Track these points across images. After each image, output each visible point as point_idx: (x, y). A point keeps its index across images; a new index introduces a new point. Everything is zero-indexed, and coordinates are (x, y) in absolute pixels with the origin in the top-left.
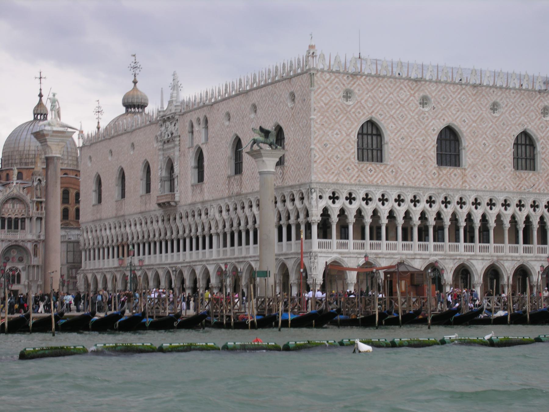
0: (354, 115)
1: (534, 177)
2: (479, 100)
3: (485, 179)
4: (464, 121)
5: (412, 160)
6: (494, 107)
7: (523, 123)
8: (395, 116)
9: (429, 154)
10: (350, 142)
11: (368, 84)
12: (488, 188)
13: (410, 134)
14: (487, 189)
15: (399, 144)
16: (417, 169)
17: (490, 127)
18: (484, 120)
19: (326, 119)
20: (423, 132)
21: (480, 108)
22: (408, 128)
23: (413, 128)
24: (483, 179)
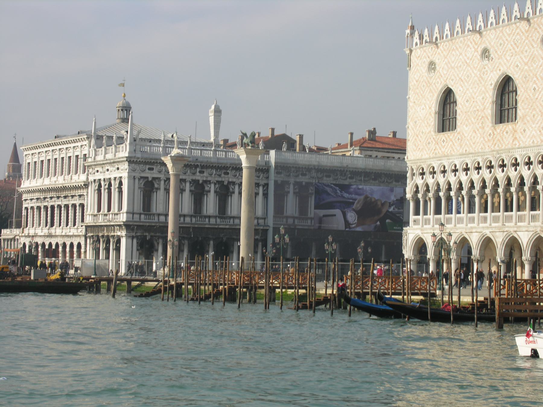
0: (434, 86)
2: (531, 37)
4: (517, 66)
5: (473, 123)
8: (462, 78)
9: (487, 113)
10: (431, 115)
11: (445, 50)
12: (536, 142)
13: (473, 94)
14: (535, 145)
15: (465, 108)
16: (477, 132)
18: (535, 59)
19: (417, 96)
20: (483, 89)
22: (471, 88)
23: (475, 88)
24: (531, 133)
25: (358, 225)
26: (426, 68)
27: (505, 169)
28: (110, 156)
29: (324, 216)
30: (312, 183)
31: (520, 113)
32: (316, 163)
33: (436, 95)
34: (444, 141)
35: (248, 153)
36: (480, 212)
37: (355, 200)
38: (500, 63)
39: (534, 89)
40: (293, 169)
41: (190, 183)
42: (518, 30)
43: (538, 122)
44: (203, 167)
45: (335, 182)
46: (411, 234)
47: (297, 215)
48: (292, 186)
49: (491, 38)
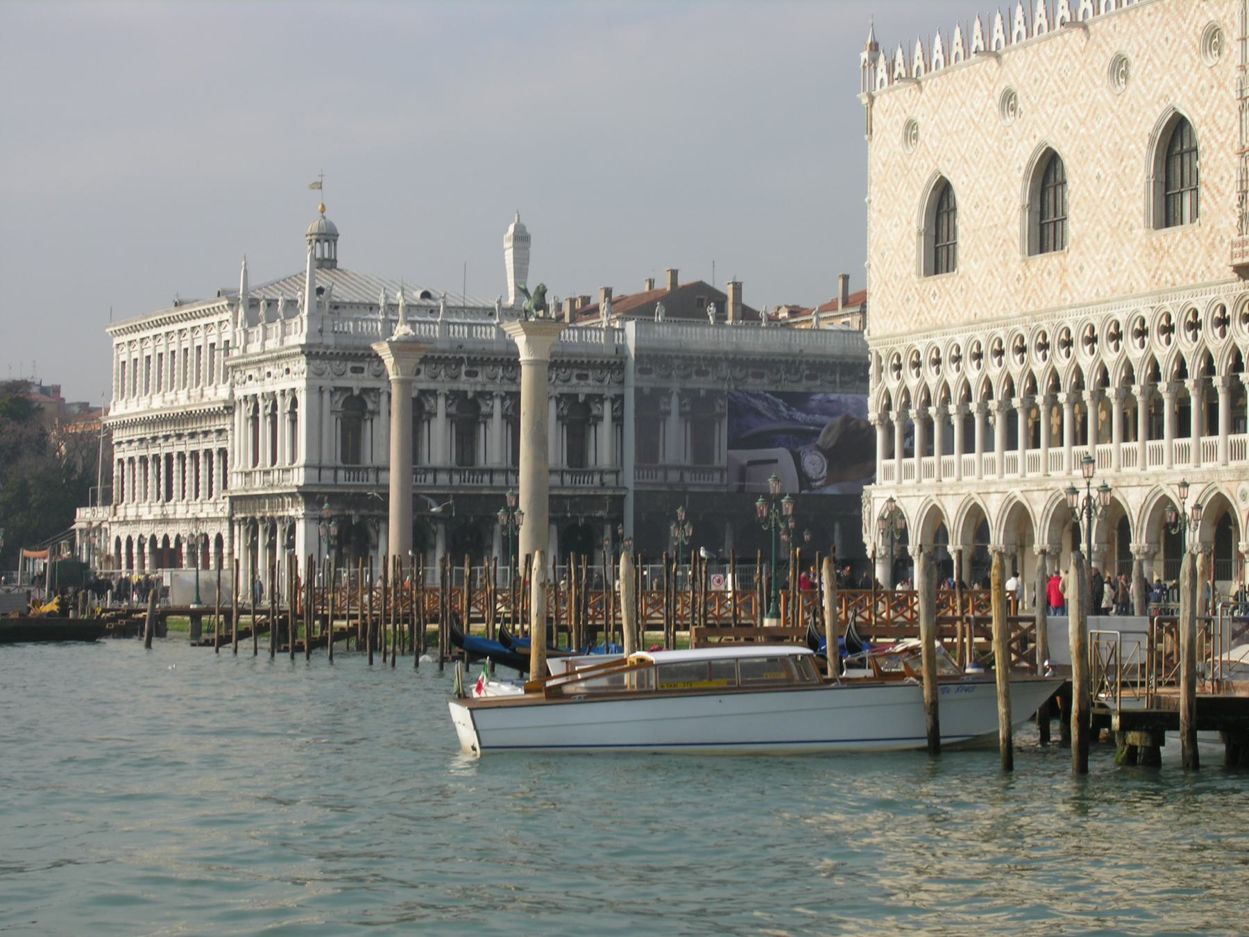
1: (1185, 241)
2: (1091, 63)
3: (1098, 272)
4: (1067, 128)
6: (1119, 67)
7: (1167, 92)
8: (967, 156)
11: (934, 95)
17: (1109, 127)
20: (1005, 179)
21: (1093, 81)
25: (829, 481)
26: (901, 135)
27: (1048, 353)
28: (272, 344)
29: (751, 463)
30: (719, 393)
31: (1073, 228)
32: (728, 348)
33: (919, 194)
34: (935, 295)
35: (528, 331)
36: (1027, 447)
37: (822, 426)
38: (1035, 122)
39: (1098, 177)
40: (676, 362)
41: (447, 398)
42: (1067, 49)
43: (1106, 249)
44: (473, 362)
45: (773, 388)
46: (876, 499)
47: (688, 462)
48: (675, 400)
49: (1018, 67)
